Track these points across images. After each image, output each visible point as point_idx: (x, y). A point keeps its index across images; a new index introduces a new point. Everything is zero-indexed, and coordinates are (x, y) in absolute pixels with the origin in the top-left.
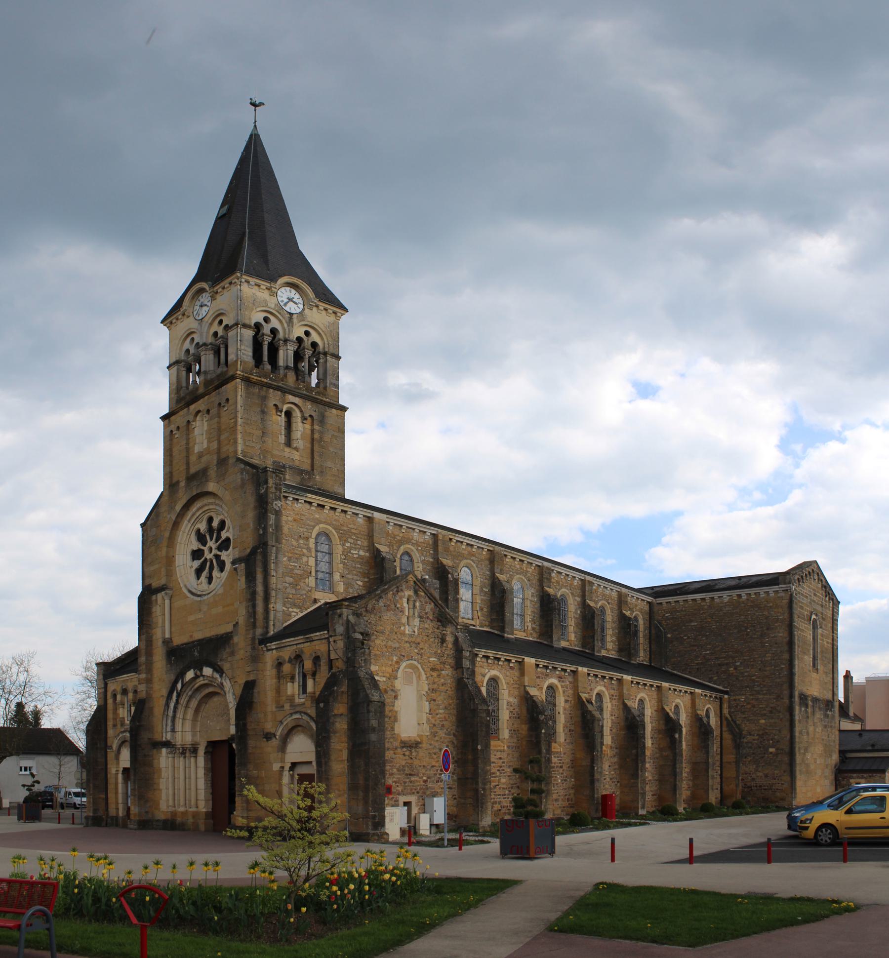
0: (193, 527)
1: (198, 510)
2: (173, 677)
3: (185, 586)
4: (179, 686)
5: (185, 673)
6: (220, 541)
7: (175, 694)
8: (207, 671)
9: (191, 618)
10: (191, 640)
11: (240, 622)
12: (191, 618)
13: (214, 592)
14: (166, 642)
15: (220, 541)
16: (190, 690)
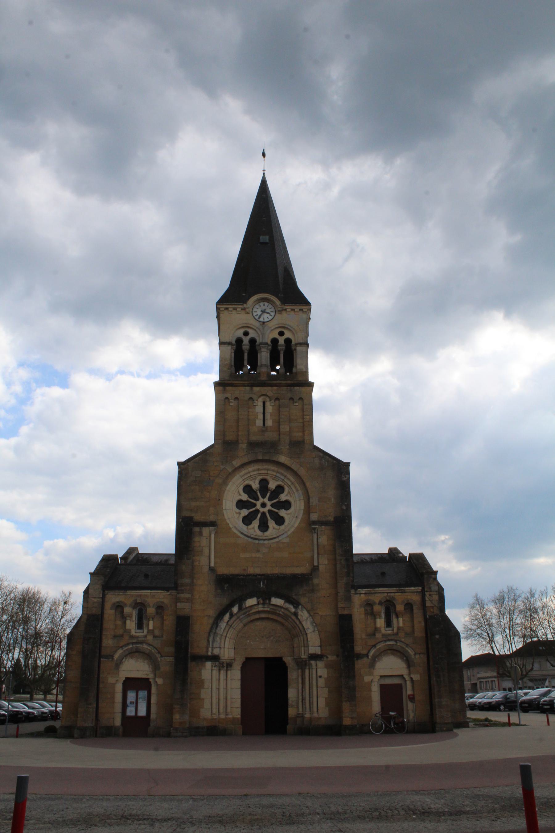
0: (243, 482)
1: (254, 471)
2: (225, 601)
3: (235, 527)
4: (235, 609)
5: (245, 600)
6: (275, 501)
7: (227, 616)
8: (277, 601)
9: (242, 555)
10: (245, 573)
11: (321, 567)
12: (242, 555)
13: (277, 540)
14: (212, 570)
15: (275, 501)
16: (244, 614)
